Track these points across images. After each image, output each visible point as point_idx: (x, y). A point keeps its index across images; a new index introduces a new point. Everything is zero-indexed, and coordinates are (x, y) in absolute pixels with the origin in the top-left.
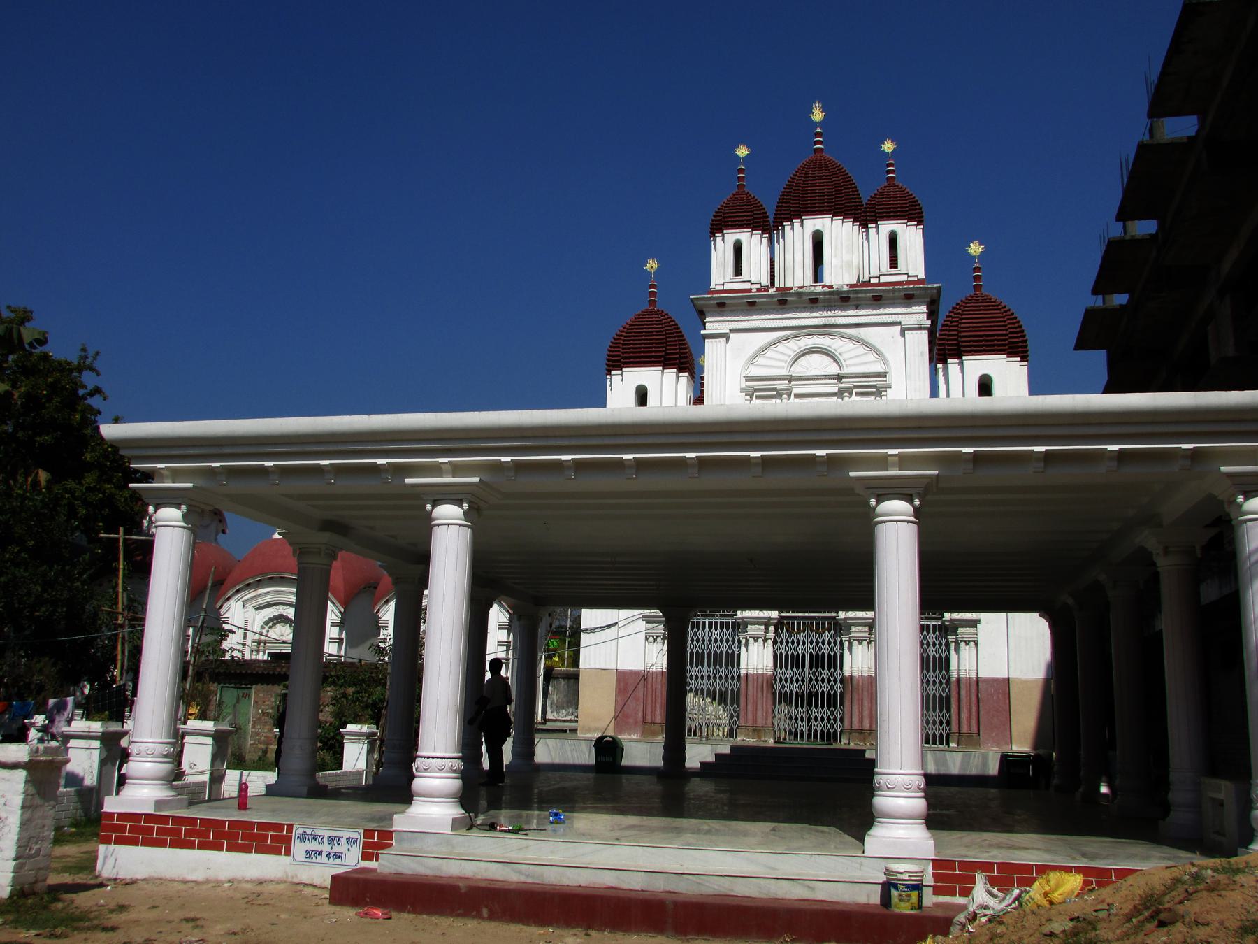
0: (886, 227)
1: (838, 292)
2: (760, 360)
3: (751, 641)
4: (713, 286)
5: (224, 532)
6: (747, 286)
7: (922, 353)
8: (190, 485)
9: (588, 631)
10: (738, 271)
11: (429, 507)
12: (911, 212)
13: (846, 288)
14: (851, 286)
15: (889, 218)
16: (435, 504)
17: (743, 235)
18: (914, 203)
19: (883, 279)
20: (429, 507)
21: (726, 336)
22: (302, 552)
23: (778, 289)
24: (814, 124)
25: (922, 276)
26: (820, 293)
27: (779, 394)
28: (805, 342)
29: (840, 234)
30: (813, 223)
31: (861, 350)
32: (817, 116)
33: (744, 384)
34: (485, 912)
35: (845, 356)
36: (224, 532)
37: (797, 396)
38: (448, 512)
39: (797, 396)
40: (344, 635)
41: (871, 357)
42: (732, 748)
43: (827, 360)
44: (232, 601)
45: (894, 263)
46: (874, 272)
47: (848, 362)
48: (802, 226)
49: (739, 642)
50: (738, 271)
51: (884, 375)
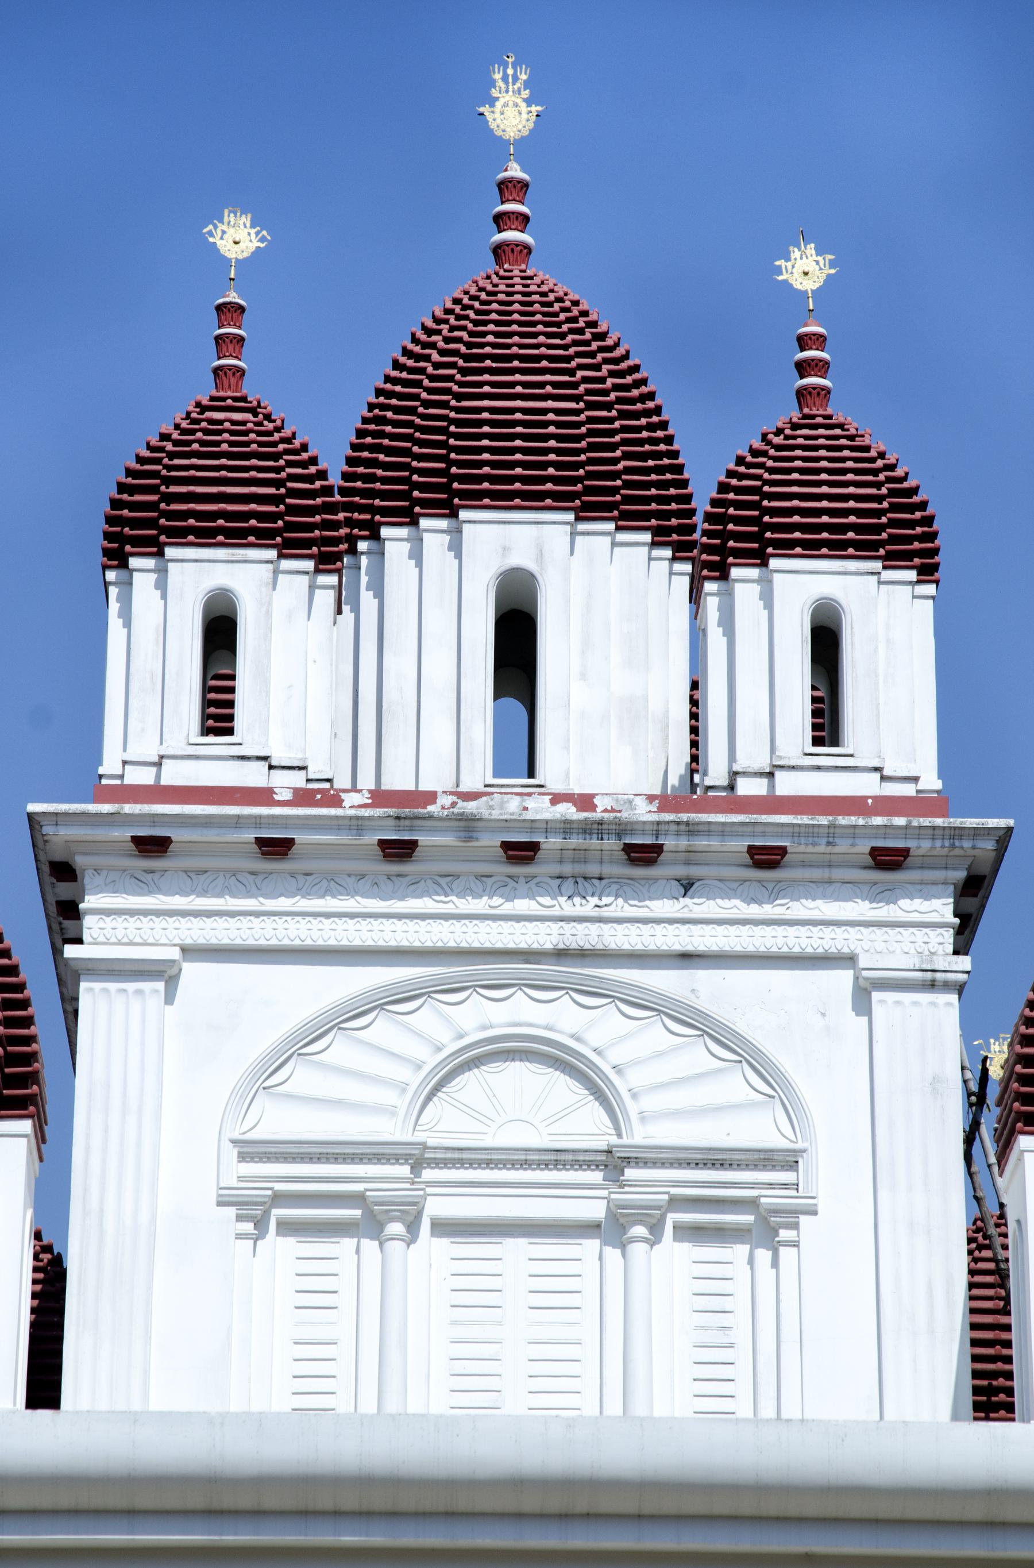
0: (802, 583)
1: (621, 829)
2: (300, 1077)
4: (110, 765)
6: (254, 776)
7: (936, 1082)
10: (218, 716)
12: (897, 532)
13: (644, 812)
14: (665, 801)
15: (812, 548)
17: (245, 573)
18: (905, 498)
19: (787, 785)
21: (164, 973)
23: (380, 797)
24: (498, 147)
25: (931, 781)
26: (548, 827)
27: (371, 1220)
28: (480, 1015)
29: (605, 589)
30: (500, 540)
31: (699, 1055)
32: (511, 114)
33: (236, 1172)
35: (636, 1078)
37: (444, 1228)
39: (444, 1228)
41: (736, 1085)
43: (563, 1088)
45: (827, 724)
46: (753, 755)
47: (650, 1103)
48: (456, 548)
50: (218, 716)
51: (788, 1160)
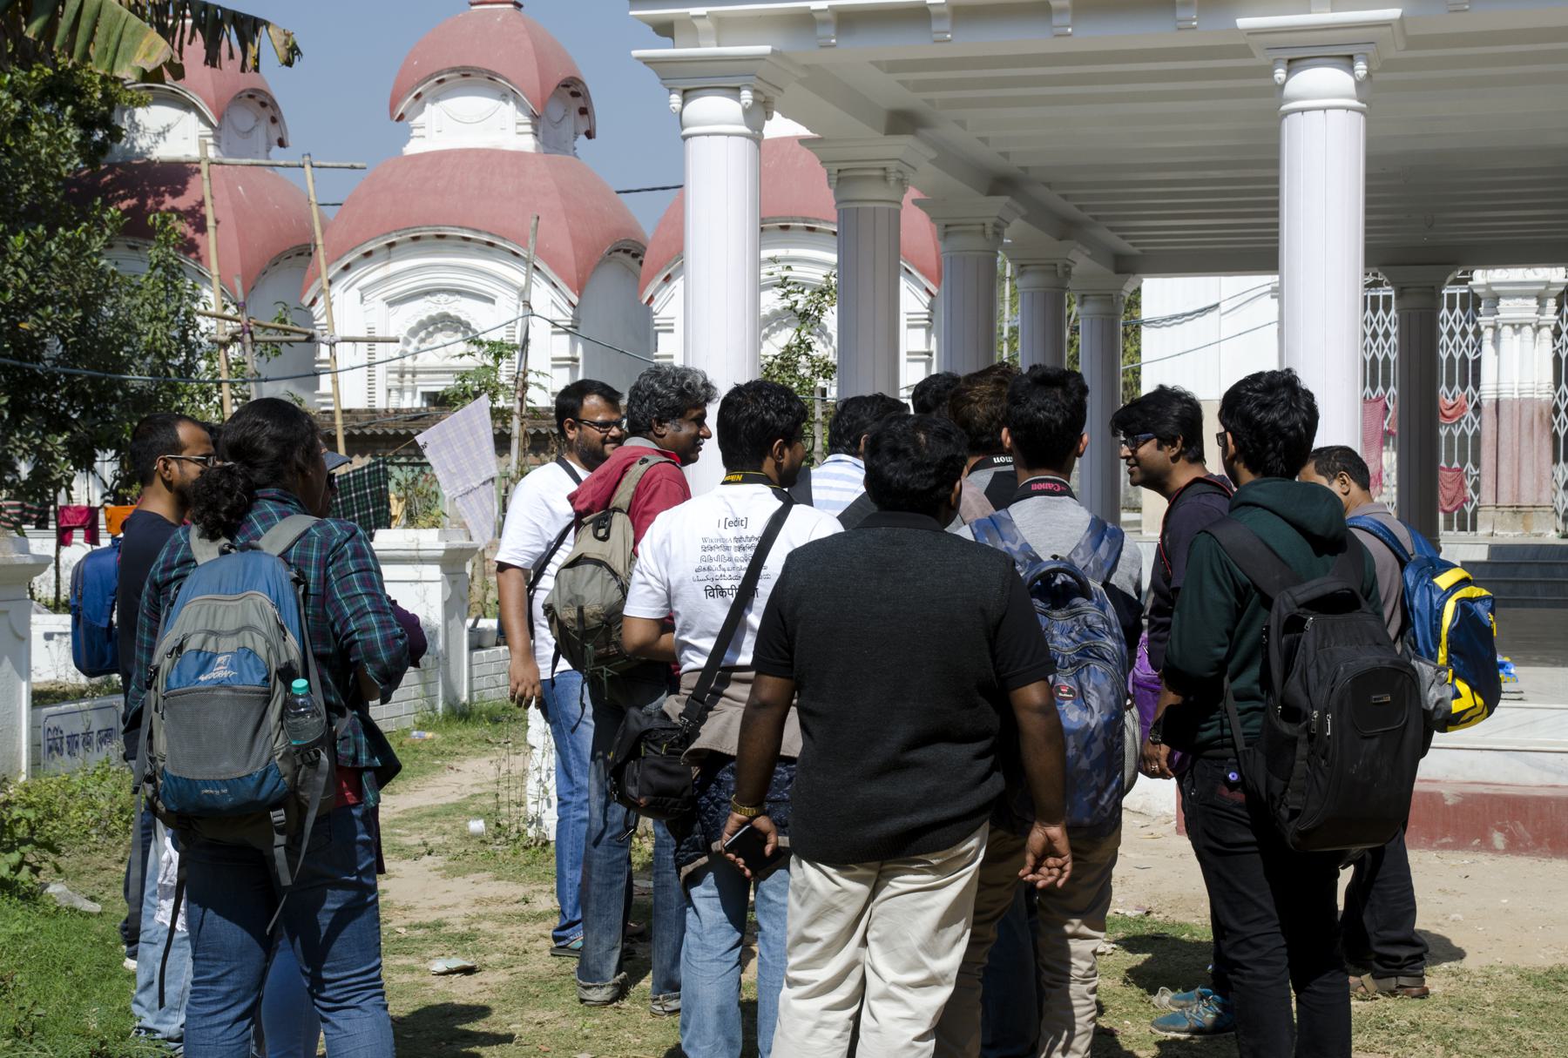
3: (1507, 331)
5: (281, 143)
8: (765, 49)
9: (1152, 323)
11: (1280, 74)
16: (1293, 65)
20: (1280, 74)
22: (843, 179)
34: (1499, 839)
36: (281, 143)
38: (1322, 85)
40: (579, 353)
42: (1494, 550)
44: (336, 290)
49: (1478, 333)
